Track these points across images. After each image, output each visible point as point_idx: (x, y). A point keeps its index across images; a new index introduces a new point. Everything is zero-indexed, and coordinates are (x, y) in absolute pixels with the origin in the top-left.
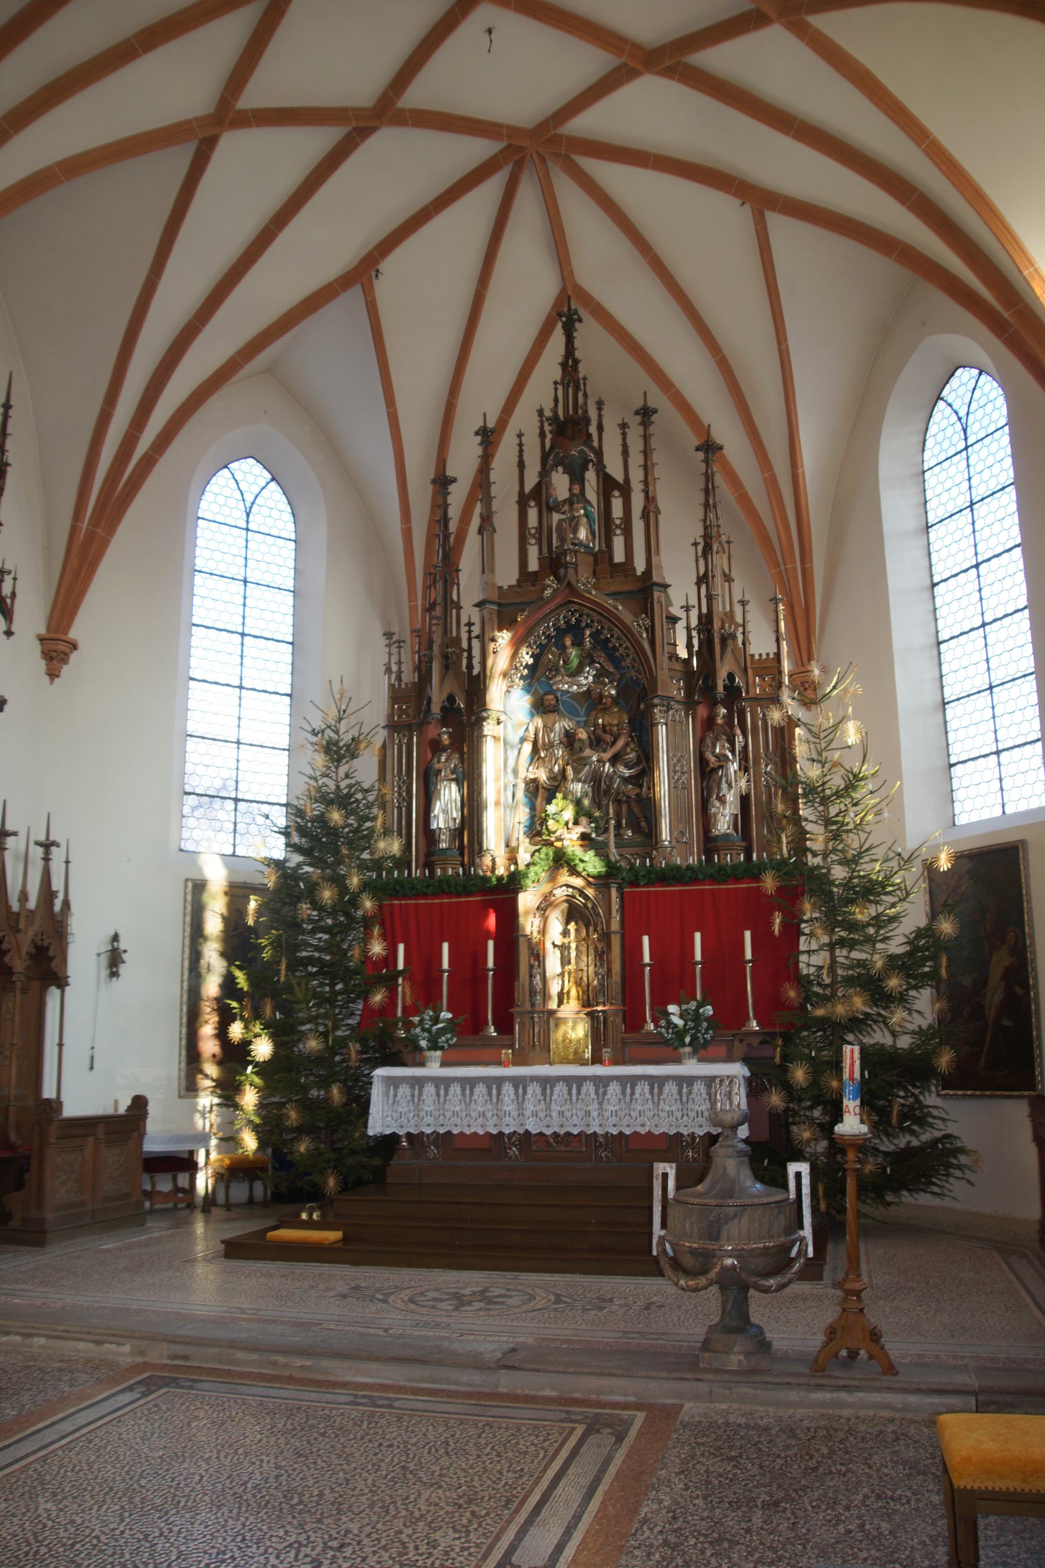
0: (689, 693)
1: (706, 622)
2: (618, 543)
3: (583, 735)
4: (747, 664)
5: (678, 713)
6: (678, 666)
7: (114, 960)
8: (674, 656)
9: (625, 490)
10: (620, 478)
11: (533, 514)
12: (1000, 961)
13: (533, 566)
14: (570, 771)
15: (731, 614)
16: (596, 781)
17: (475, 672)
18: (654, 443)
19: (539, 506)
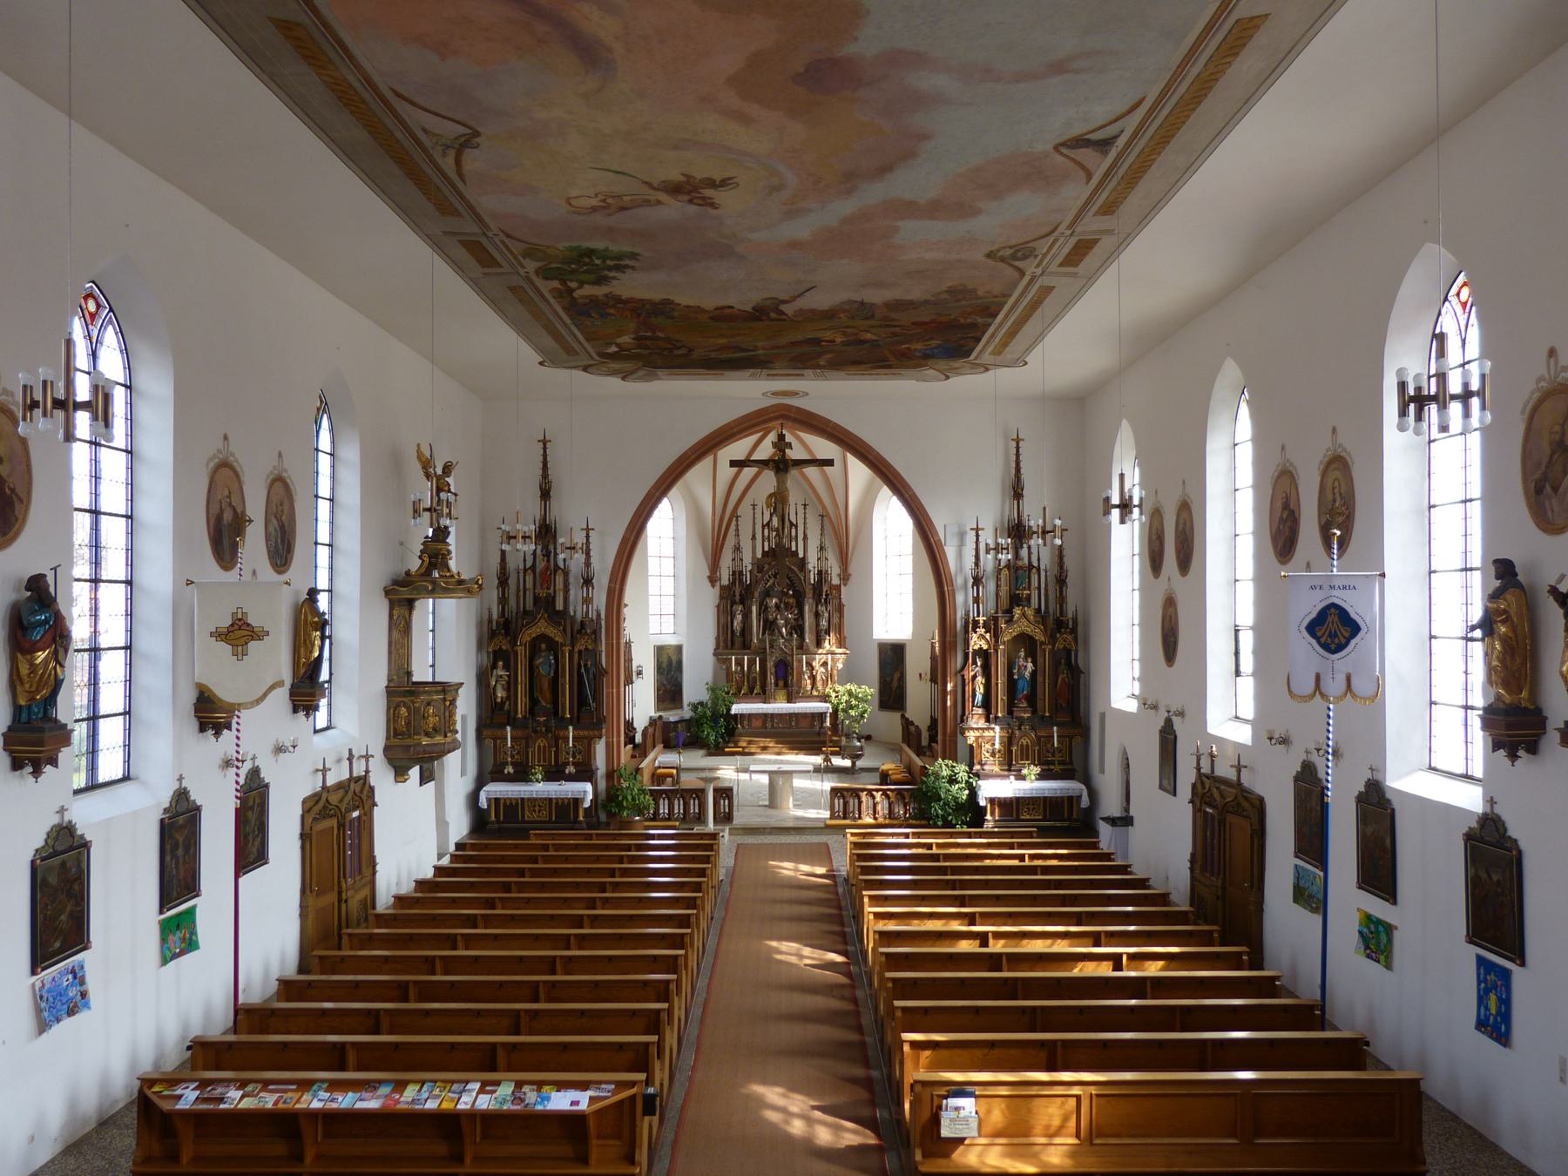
0: (814, 595)
1: (820, 573)
2: (794, 544)
3: (782, 606)
4: (832, 587)
5: (811, 601)
6: (811, 587)
7: (640, 673)
8: (810, 583)
9: (796, 527)
10: (795, 523)
11: (766, 531)
12: (896, 676)
13: (766, 549)
14: (779, 617)
15: (827, 571)
16: (787, 620)
17: (748, 582)
18: (807, 516)
19: (768, 528)
